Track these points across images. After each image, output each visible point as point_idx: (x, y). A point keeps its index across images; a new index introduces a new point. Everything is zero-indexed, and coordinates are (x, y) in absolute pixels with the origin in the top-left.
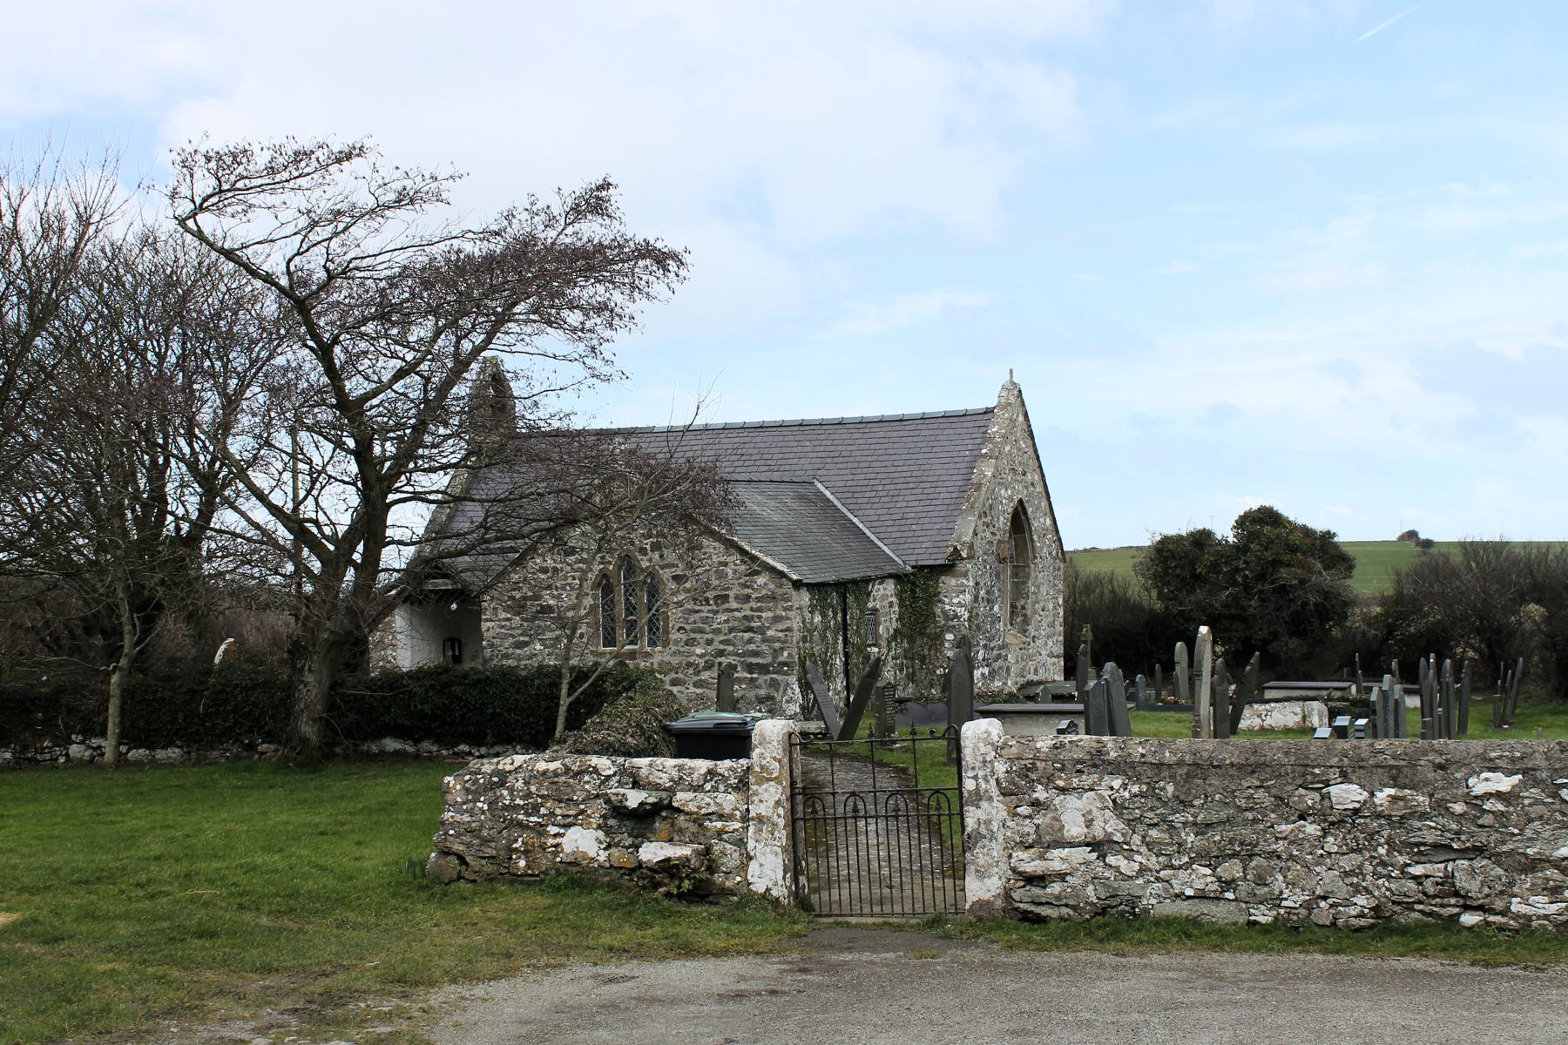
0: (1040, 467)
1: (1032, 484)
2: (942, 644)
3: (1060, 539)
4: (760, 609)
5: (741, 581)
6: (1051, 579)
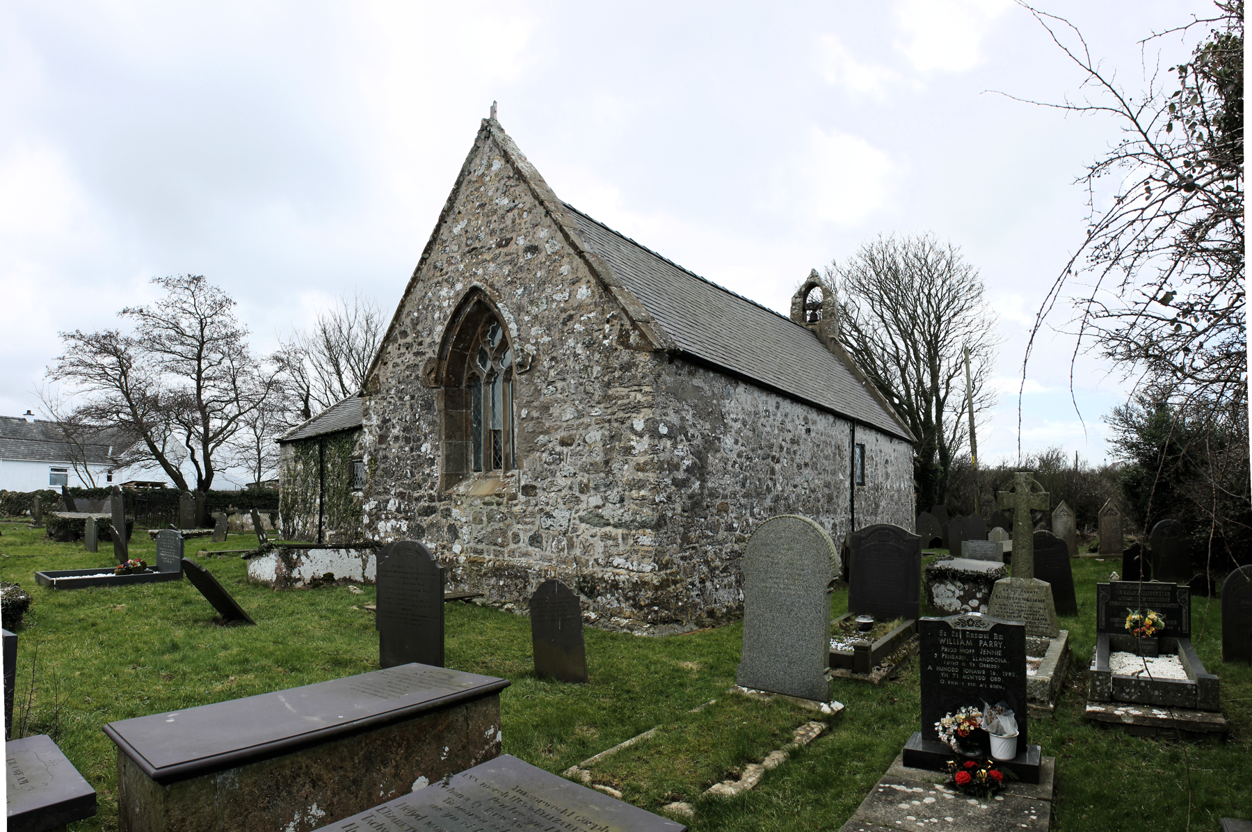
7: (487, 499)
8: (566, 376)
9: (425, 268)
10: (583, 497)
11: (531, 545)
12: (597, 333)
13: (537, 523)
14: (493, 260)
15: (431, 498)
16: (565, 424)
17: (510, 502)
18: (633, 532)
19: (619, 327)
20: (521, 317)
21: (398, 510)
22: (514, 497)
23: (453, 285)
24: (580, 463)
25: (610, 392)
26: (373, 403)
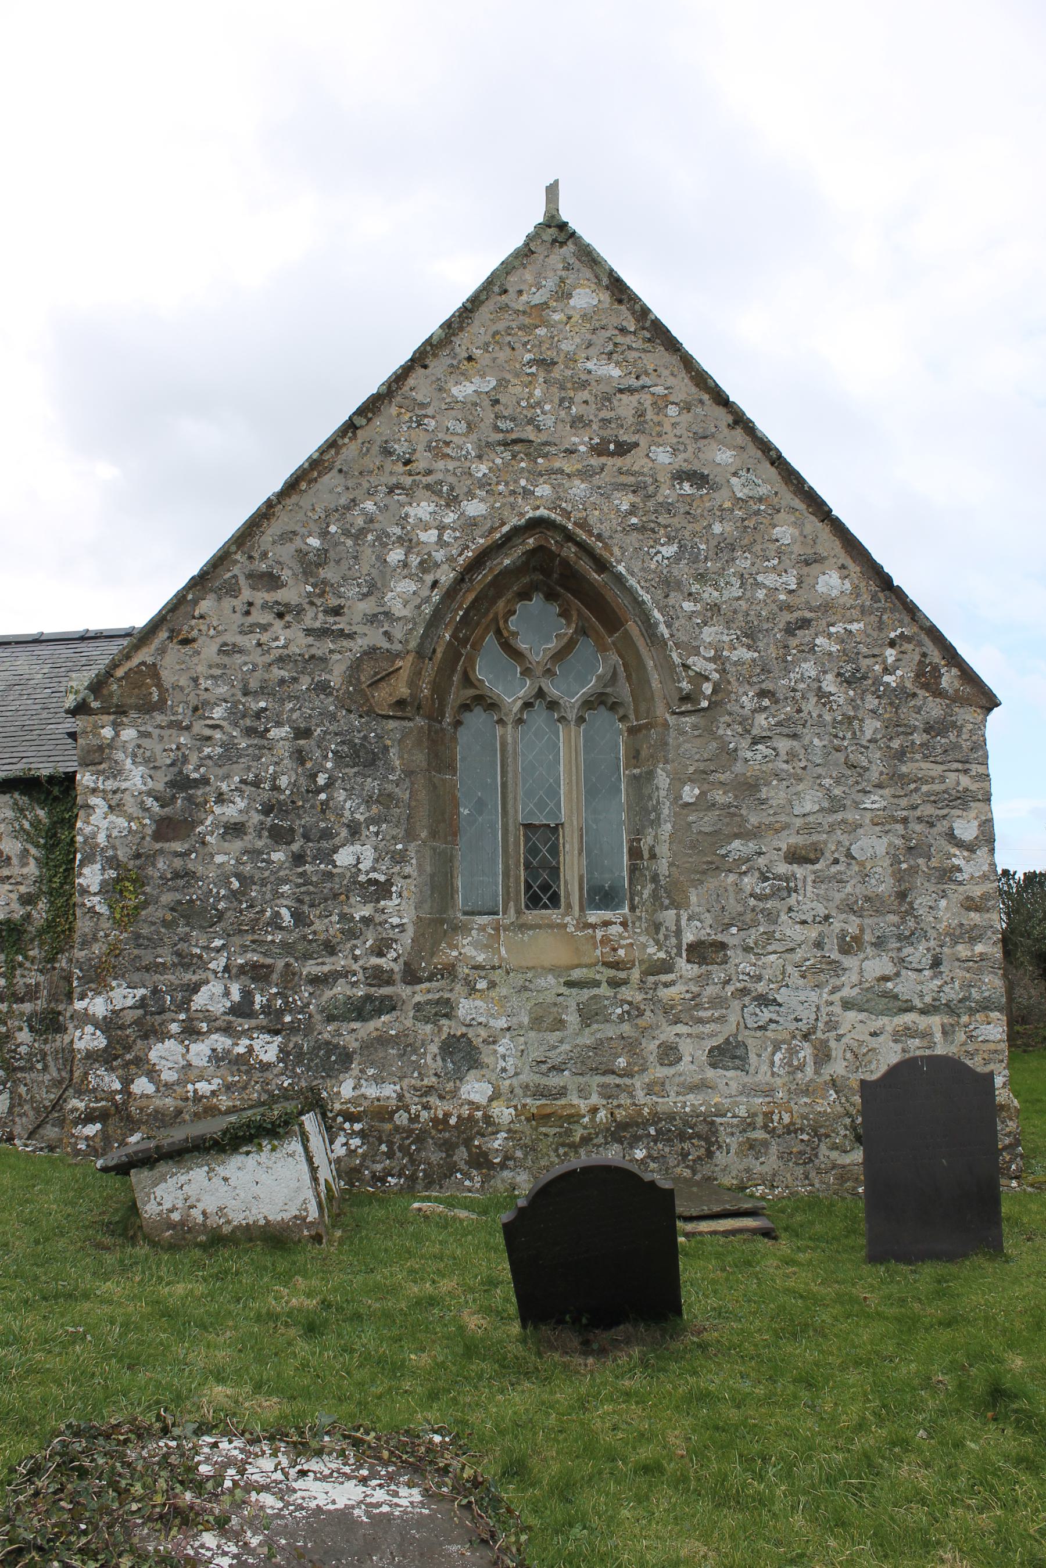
0: (740, 421)
7: (576, 974)
8: (799, 729)
9: (351, 449)
10: (848, 961)
11: (714, 1066)
12: (869, 661)
13: (733, 1018)
14: (585, 474)
15: (380, 978)
16: (798, 822)
17: (651, 979)
18: (965, 1019)
19: (917, 658)
20: (671, 601)
21: (242, 1009)
22: (666, 967)
23: (452, 501)
24: (838, 897)
25: (904, 769)
26: (129, 734)
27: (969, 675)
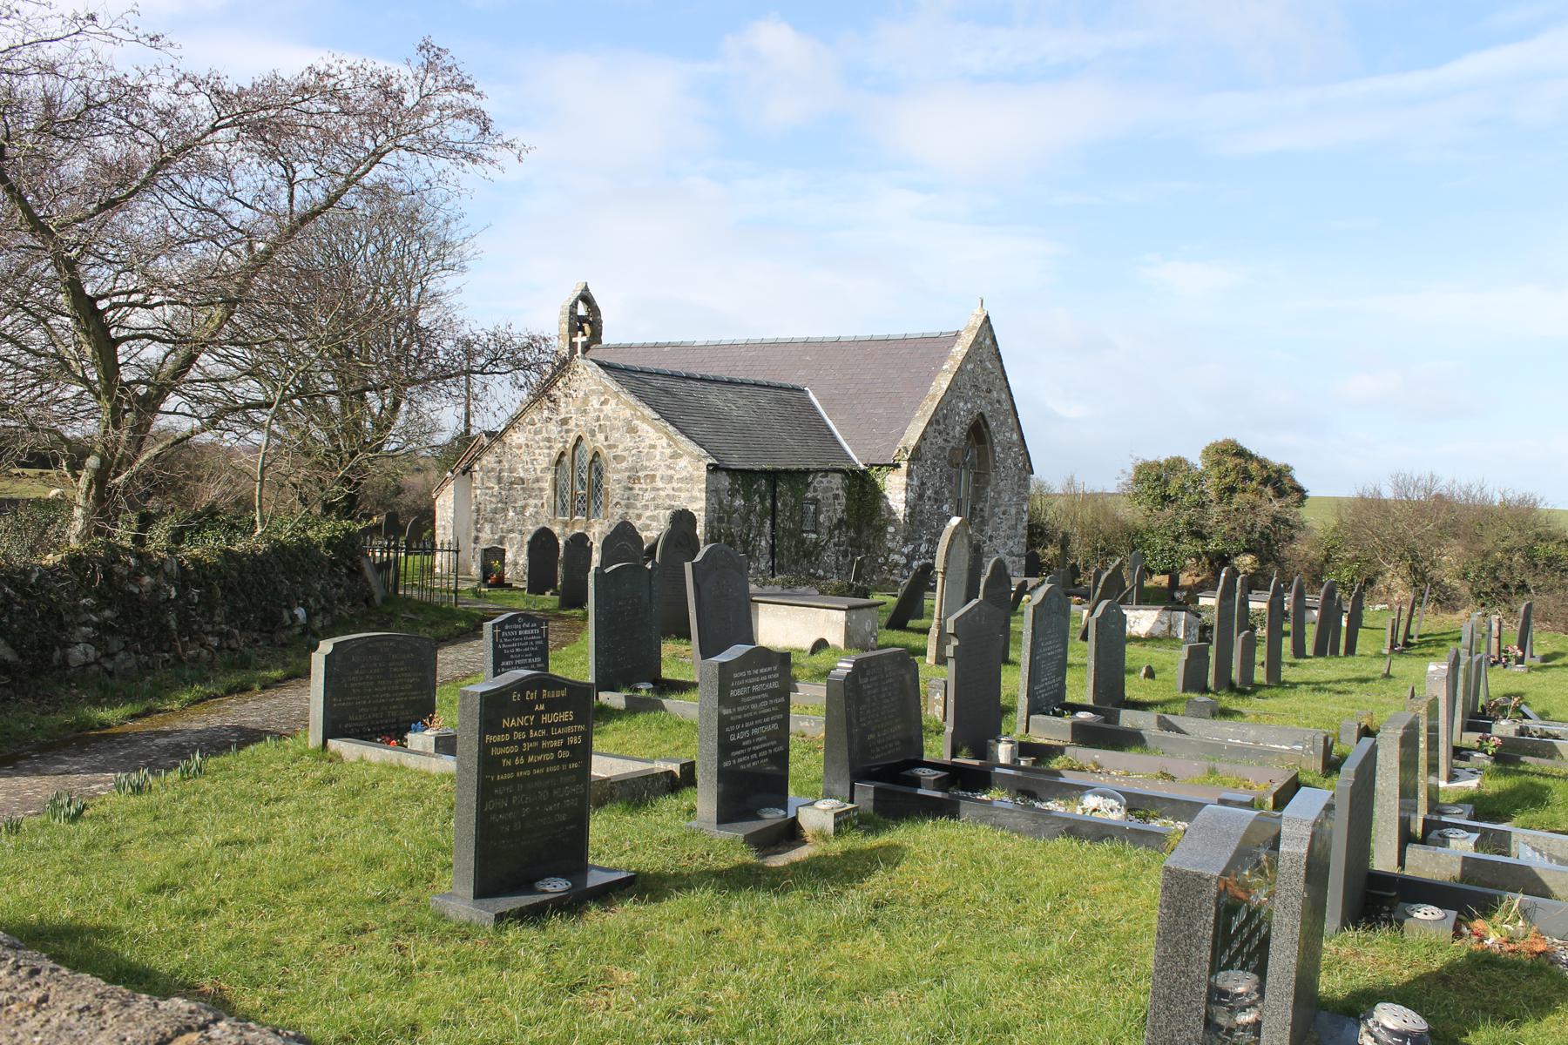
1: (998, 401)
2: (885, 536)
3: (1028, 453)
4: (680, 490)
5: (666, 463)
6: (1016, 487)
23: (966, 403)
27: (1031, 465)
